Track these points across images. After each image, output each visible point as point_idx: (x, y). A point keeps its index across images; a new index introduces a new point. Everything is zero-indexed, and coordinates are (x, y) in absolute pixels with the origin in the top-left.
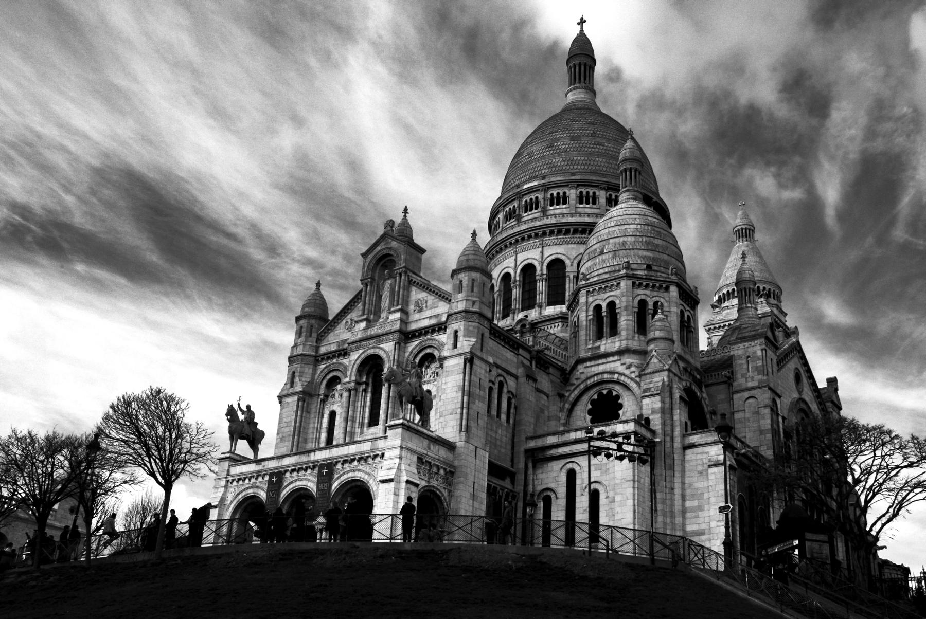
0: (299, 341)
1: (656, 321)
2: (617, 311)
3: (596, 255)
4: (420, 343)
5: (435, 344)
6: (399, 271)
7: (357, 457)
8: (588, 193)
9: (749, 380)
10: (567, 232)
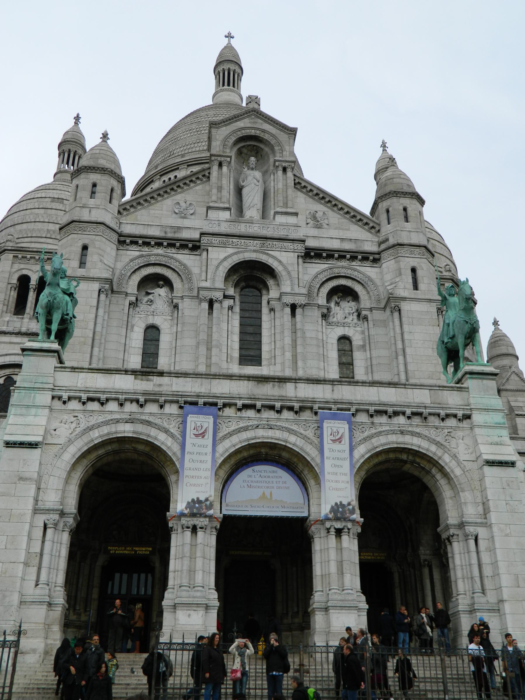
0: (92, 202)
1: (503, 336)
5: (355, 274)
6: (284, 164)
7: (408, 412)
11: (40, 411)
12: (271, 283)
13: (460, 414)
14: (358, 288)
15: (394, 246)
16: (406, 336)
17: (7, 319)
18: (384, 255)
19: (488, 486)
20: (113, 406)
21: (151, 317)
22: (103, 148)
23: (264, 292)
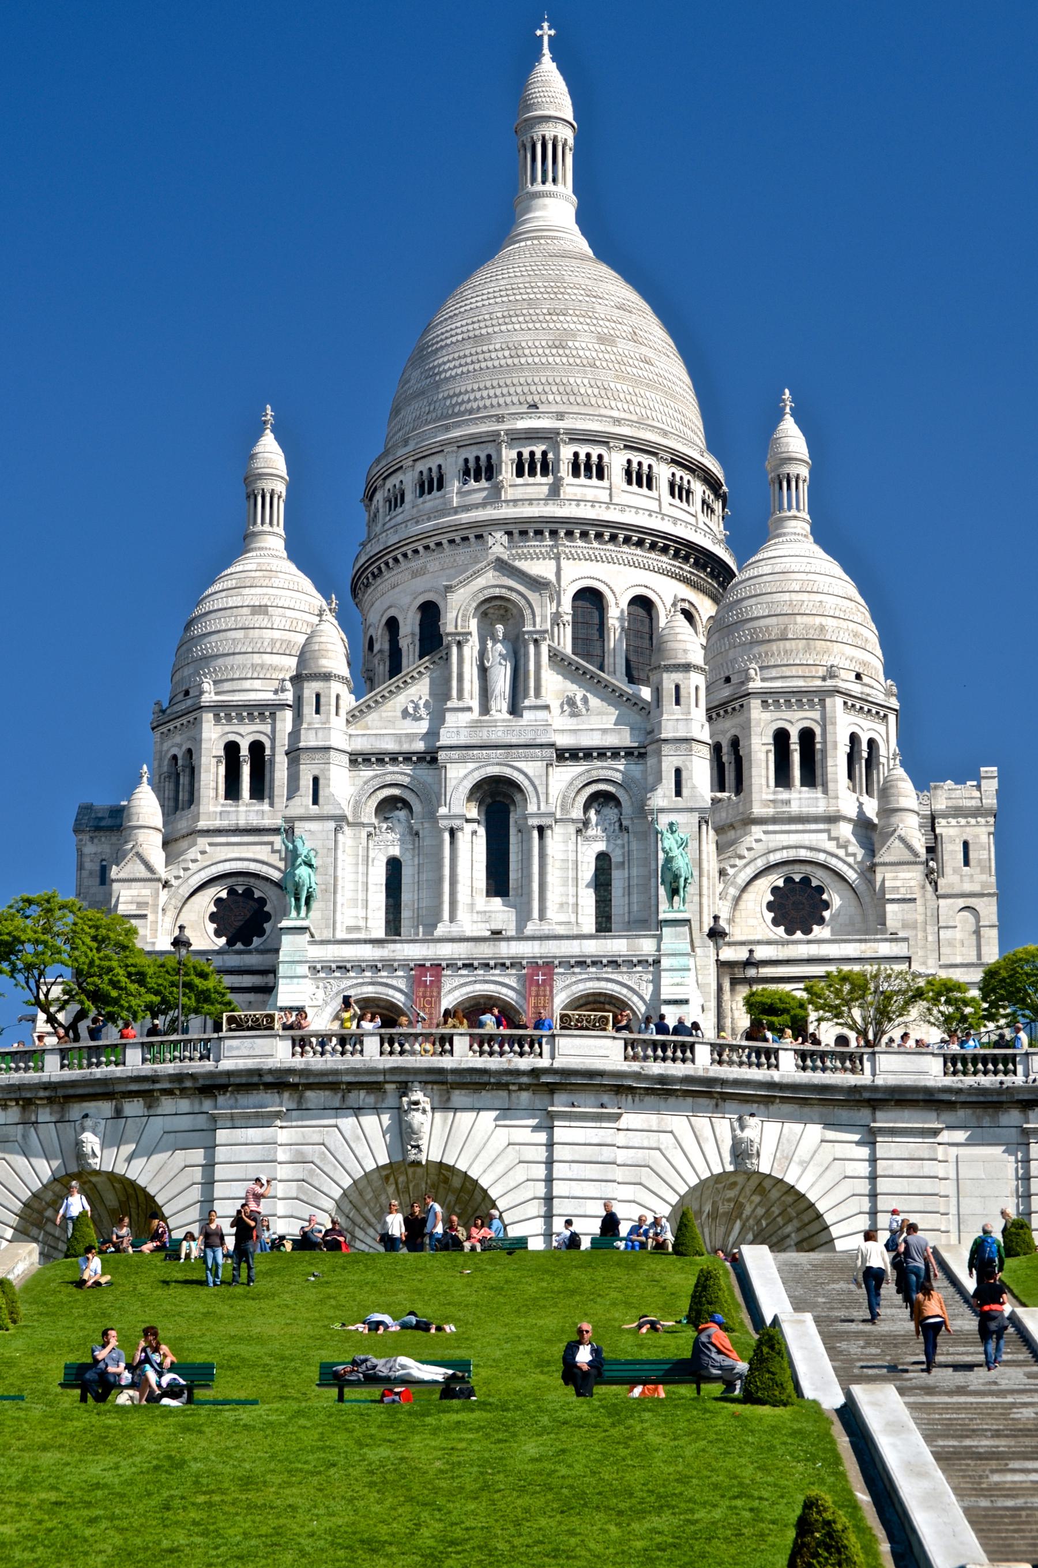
1: (897, 780)
2: (818, 746)
3: (773, 637)
4: (588, 771)
7: (605, 961)
8: (640, 464)
9: (966, 879)
10: (613, 538)
12: (518, 797)
13: (651, 960)
17: (219, 809)
22: (322, 639)
23: (512, 808)
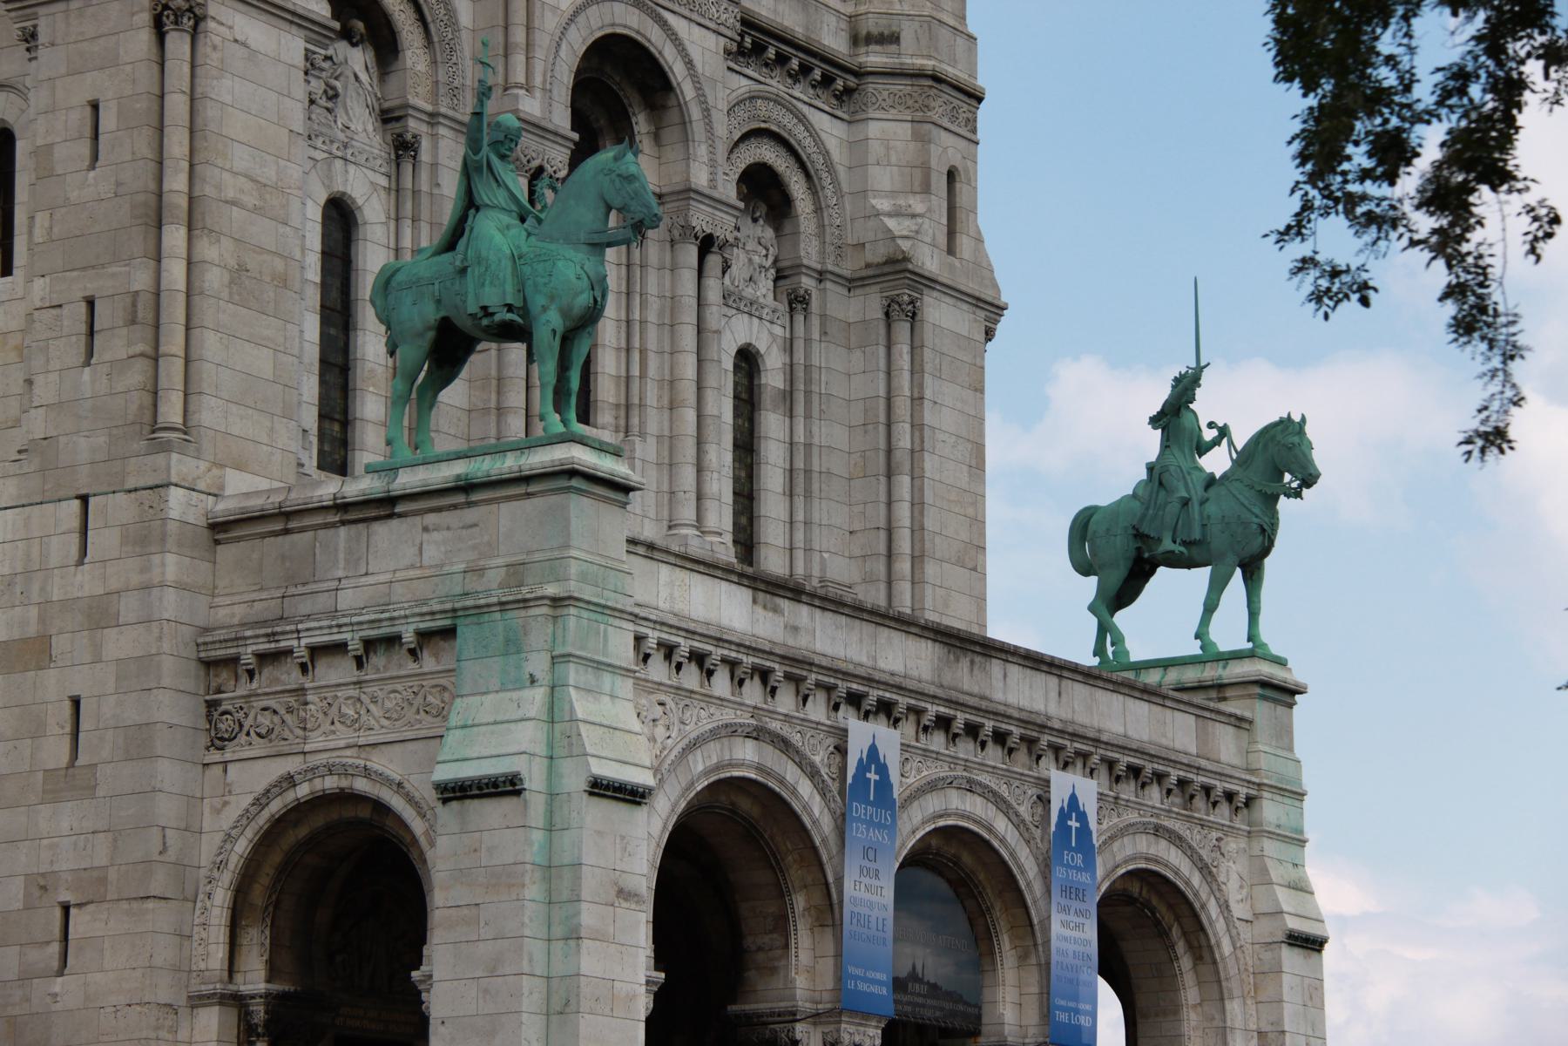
4: (752, 98)
5: (799, 135)
11: (619, 680)
12: (641, 124)
13: (1243, 791)
14: (797, 187)
15: (917, 75)
16: (929, 417)
18: (872, 86)
19: (1285, 998)
20: (721, 684)
21: (339, 164)
